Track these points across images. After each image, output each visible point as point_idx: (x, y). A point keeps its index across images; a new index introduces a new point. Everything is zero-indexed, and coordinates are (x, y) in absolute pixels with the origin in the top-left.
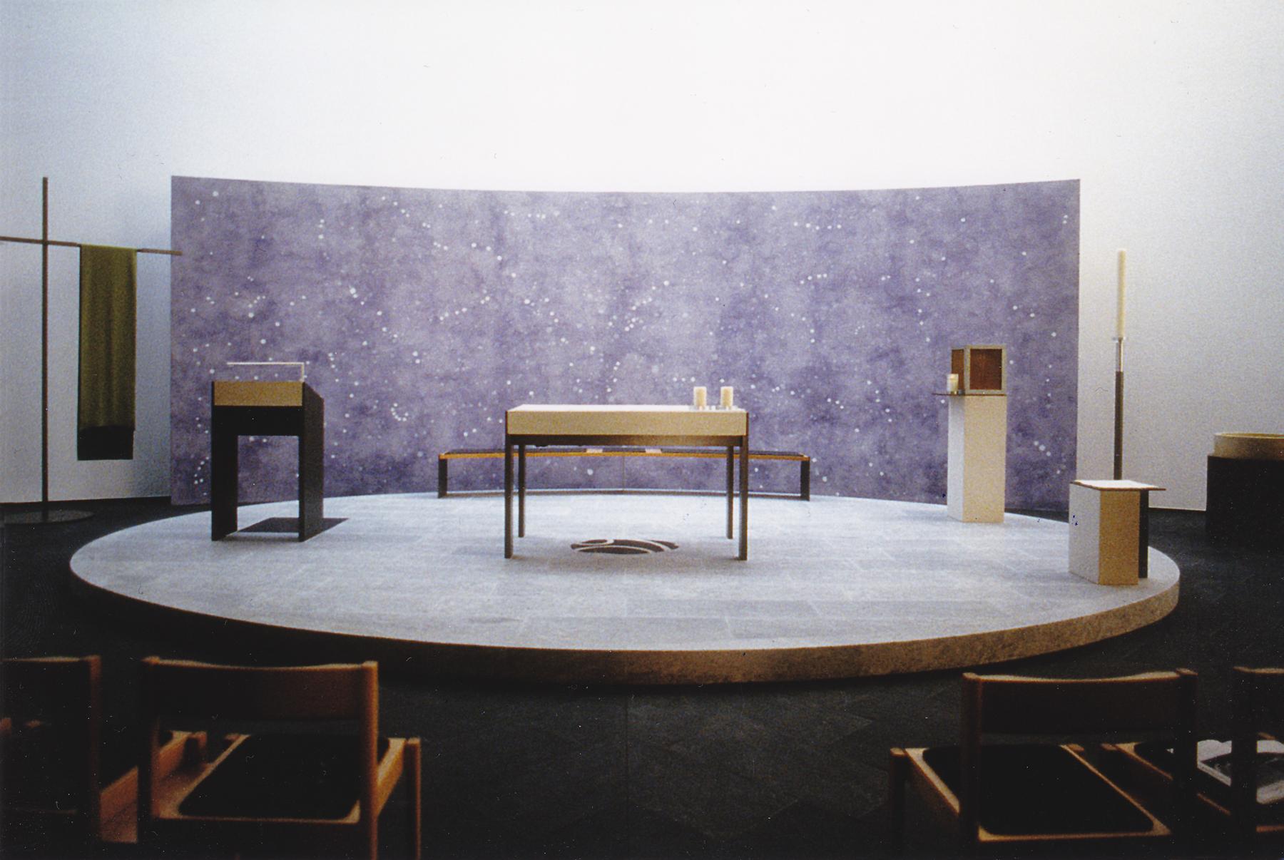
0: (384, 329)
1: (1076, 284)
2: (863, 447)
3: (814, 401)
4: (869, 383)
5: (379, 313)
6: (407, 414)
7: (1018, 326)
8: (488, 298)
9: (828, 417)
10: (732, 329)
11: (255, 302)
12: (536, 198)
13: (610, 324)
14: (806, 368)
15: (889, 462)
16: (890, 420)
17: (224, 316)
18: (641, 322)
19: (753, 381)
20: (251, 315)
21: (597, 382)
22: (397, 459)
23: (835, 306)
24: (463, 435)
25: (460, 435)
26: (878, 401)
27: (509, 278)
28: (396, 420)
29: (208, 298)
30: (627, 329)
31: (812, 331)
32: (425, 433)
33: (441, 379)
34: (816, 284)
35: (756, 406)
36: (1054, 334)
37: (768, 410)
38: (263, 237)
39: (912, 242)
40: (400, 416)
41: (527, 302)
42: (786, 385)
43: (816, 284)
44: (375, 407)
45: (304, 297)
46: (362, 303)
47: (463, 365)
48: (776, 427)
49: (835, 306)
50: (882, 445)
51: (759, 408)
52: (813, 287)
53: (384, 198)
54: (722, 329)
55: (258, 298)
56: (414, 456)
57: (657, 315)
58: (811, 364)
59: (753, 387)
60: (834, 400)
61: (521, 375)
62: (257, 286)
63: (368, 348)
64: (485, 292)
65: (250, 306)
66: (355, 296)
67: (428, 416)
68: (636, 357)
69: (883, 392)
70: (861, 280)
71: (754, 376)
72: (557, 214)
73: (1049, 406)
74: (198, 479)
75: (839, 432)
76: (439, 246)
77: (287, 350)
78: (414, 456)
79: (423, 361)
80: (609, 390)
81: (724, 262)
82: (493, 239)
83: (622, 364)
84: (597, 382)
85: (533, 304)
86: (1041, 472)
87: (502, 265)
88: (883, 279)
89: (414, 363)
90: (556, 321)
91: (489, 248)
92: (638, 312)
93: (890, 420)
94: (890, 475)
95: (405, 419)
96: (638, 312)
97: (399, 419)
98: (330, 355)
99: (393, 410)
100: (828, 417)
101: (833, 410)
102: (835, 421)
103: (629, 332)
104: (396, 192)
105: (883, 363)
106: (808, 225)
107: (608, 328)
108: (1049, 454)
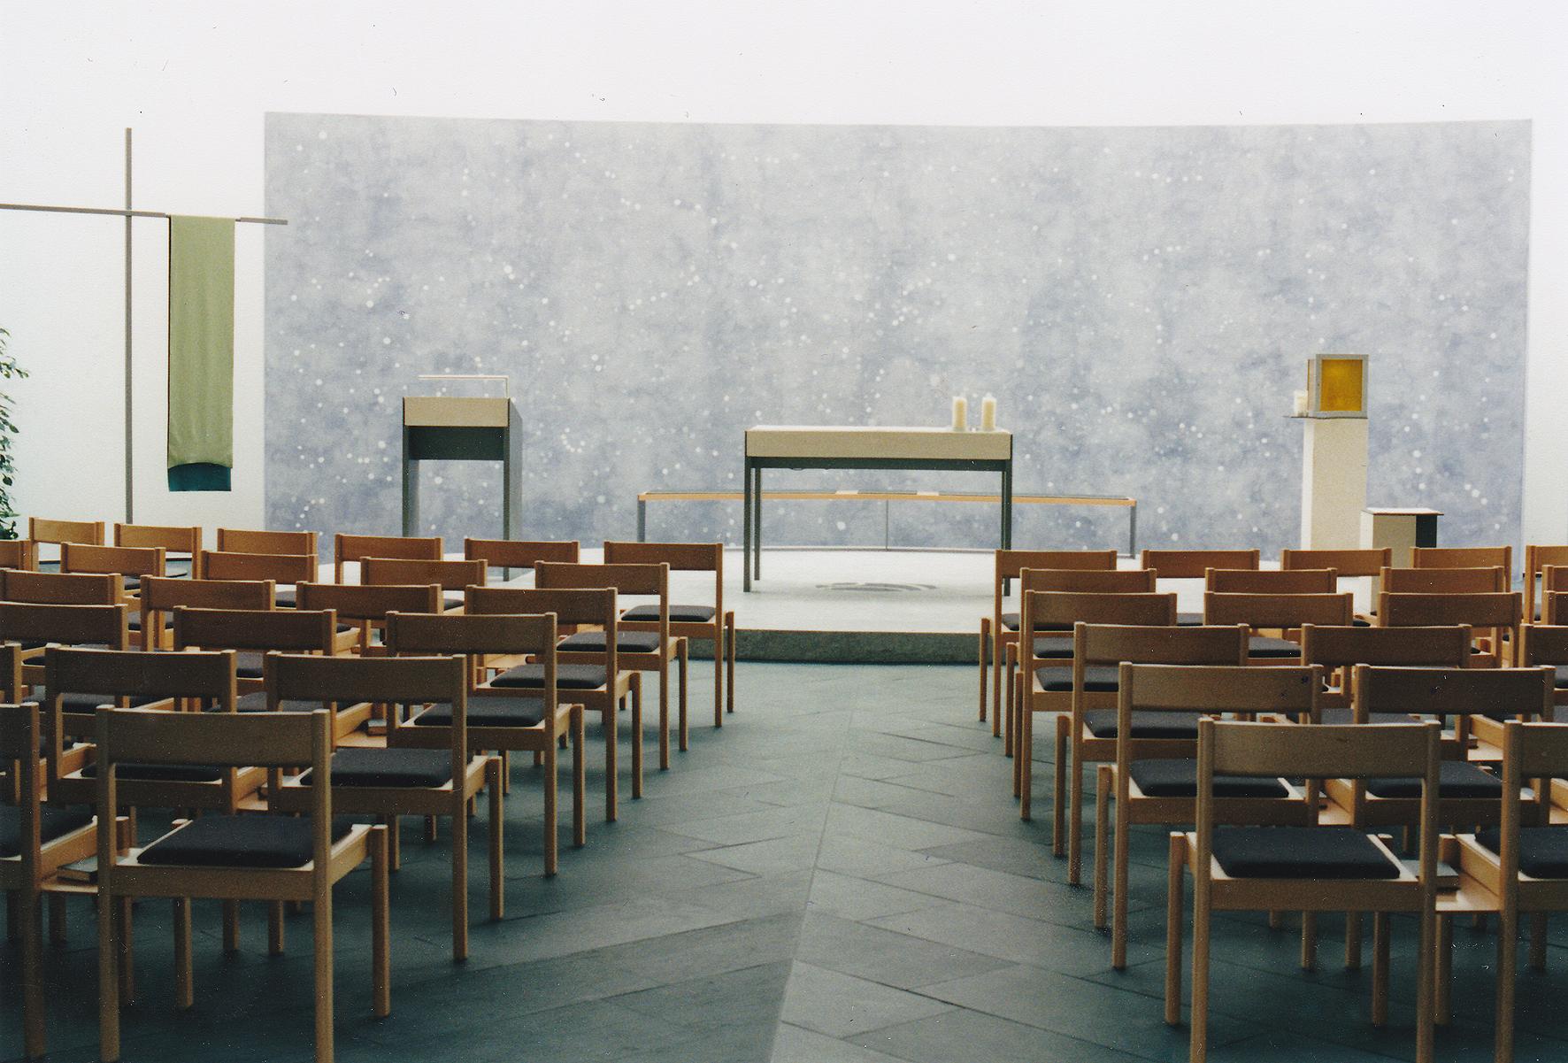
0: (552, 323)
1: (1524, 266)
2: (1229, 492)
3: (1159, 428)
4: (1238, 401)
5: (545, 301)
7: (1446, 324)
8: (697, 279)
9: (1180, 449)
10: (1046, 324)
11: (376, 285)
12: (766, 134)
13: (871, 315)
14: (1150, 380)
15: (1265, 514)
16: (1267, 454)
17: (333, 306)
18: (916, 312)
19: (1075, 398)
20: (370, 304)
21: (852, 399)
22: (570, 505)
23: (1192, 291)
24: (661, 472)
25: (658, 473)
26: (1251, 426)
27: (728, 249)
28: (568, 452)
29: (314, 281)
30: (895, 323)
31: (1159, 327)
32: (608, 469)
33: (630, 394)
34: (1165, 261)
35: (1079, 433)
36: (1493, 336)
37: (1095, 440)
38: (386, 195)
39: (1301, 201)
40: (572, 446)
41: (753, 283)
42: (1122, 405)
43: (1165, 261)
44: (539, 433)
45: (442, 279)
46: (521, 286)
47: (661, 373)
48: (1107, 463)
49: (1192, 291)
50: (1256, 489)
51: (1082, 437)
52: (1160, 265)
53: (551, 137)
54: (1031, 323)
55: (380, 280)
56: (593, 503)
57: (938, 303)
58: (1157, 374)
59: (1074, 406)
60: (1188, 426)
61: (742, 389)
62: (378, 264)
63: (530, 350)
64: (693, 268)
65: (369, 291)
66: (512, 277)
67: (614, 446)
68: (908, 363)
69: (1258, 414)
70: (1229, 255)
71: (1076, 391)
72: (796, 156)
73: (1485, 436)
75: (1195, 471)
76: (628, 203)
77: (419, 353)
78: (593, 503)
79: (605, 367)
80: (869, 410)
81: (1035, 228)
82: (705, 194)
83: (887, 374)
84: (852, 399)
85: (760, 287)
86: (1474, 526)
87: (716, 230)
88: (1260, 253)
89: (593, 371)
90: (794, 310)
91: (698, 207)
92: (910, 298)
93: (1267, 454)
94: (1268, 531)
95: (580, 450)
96: (910, 298)
97: (572, 450)
98: (478, 359)
99: (563, 437)
100: (1180, 449)
101: (1188, 441)
102: (1189, 456)
103: (899, 326)
104: (567, 126)
105: (1258, 374)
106: (1155, 176)
107: (868, 321)
108: (1484, 501)
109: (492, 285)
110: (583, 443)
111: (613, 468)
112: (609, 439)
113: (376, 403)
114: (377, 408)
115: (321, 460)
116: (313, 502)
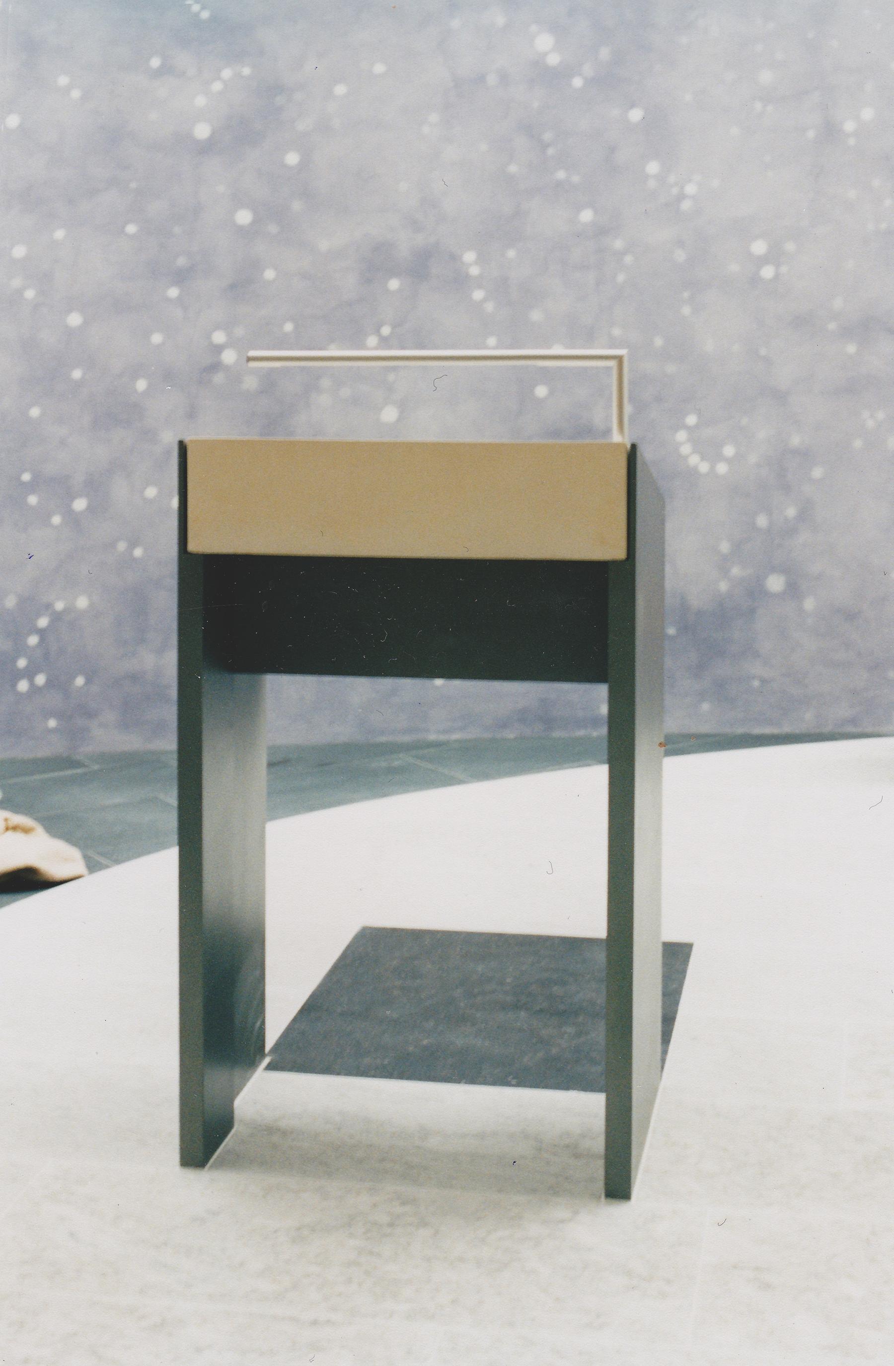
0: (653, 168)
5: (636, 115)
6: (729, 451)
11: (217, 86)
20: (202, 131)
28: (693, 472)
32: (791, 512)
46: (577, 82)
55: (227, 73)
63: (601, 231)
66: (553, 60)
74: (29, 674)
77: (324, 245)
79: (784, 269)
89: (755, 280)
95: (722, 468)
97: (704, 467)
98: (469, 257)
109: (504, 78)
110: (729, 451)
111: (805, 514)
112: (796, 441)
113: (215, 367)
114: (219, 378)
115: (80, 504)
116: (59, 606)
